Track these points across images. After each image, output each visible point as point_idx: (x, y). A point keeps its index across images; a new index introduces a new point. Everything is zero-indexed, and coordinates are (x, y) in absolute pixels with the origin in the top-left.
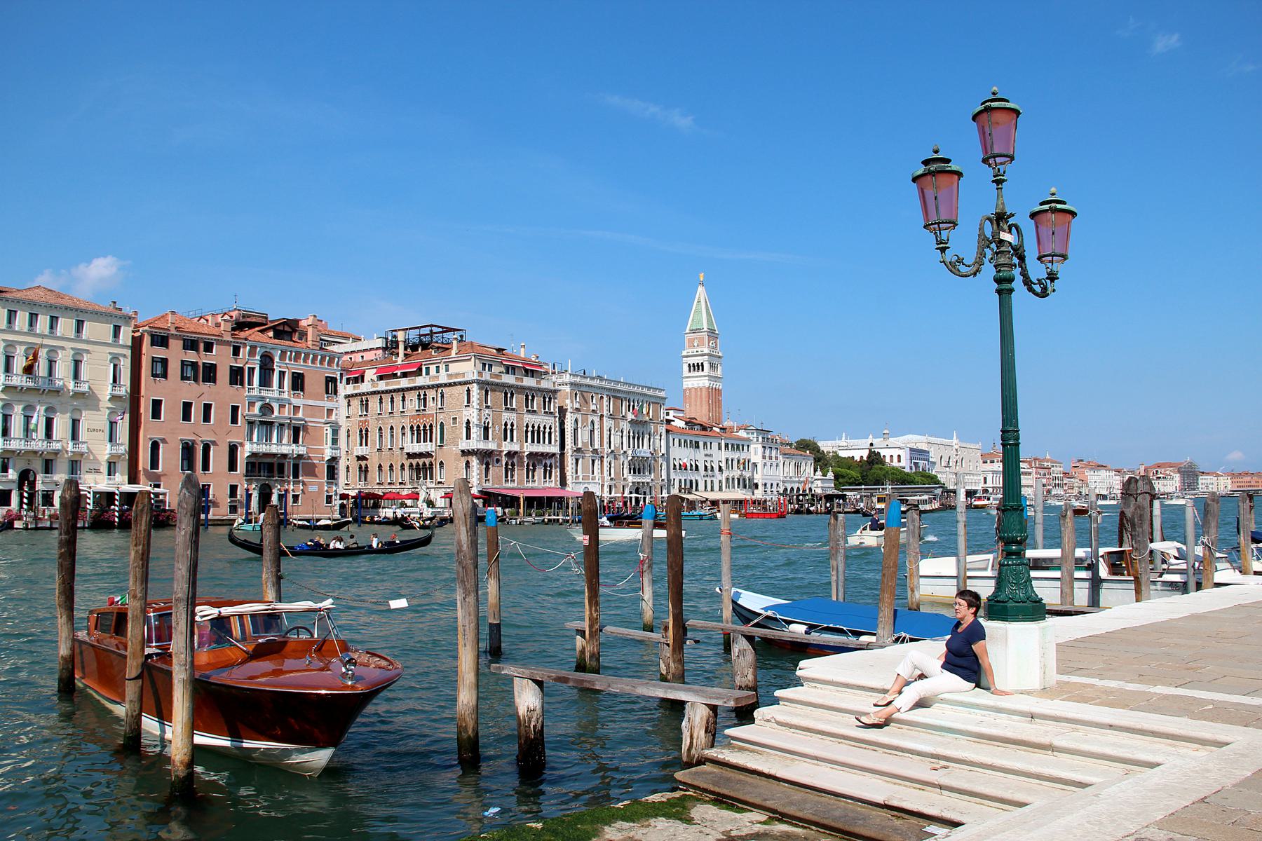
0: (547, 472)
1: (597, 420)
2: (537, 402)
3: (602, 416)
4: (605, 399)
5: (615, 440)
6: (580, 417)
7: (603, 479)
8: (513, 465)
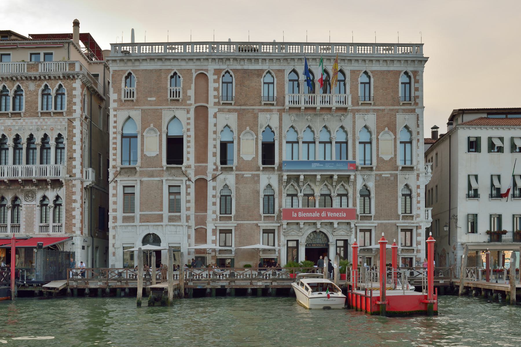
3: (201, 112)
7: (201, 221)
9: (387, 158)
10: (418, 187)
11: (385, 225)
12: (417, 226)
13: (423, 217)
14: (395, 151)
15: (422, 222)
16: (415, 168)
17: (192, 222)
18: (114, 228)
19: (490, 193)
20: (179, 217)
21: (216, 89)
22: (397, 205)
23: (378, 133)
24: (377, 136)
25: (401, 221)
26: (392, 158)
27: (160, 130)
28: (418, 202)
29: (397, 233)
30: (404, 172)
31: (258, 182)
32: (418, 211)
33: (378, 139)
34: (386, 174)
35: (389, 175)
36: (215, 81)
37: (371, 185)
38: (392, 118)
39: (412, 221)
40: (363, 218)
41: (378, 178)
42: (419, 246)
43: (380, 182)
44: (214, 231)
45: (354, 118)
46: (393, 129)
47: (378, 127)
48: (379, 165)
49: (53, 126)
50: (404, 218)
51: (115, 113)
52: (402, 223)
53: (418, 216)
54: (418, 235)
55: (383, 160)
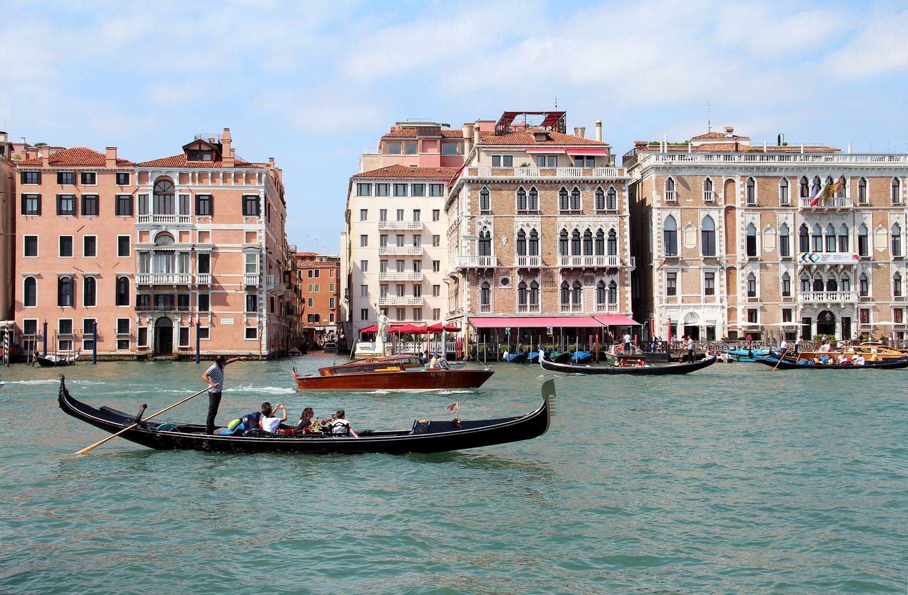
0: (606, 294)
1: (717, 215)
2: (588, 197)
3: (729, 210)
4: (738, 182)
5: (768, 244)
6: (676, 214)
8: (535, 288)
9: (881, 250)
17: (725, 304)
18: (661, 307)
20: (714, 298)
21: (742, 193)
27: (697, 227)
31: (777, 270)
36: (741, 186)
44: (743, 310)
45: (854, 216)
49: (608, 223)
51: (659, 212)
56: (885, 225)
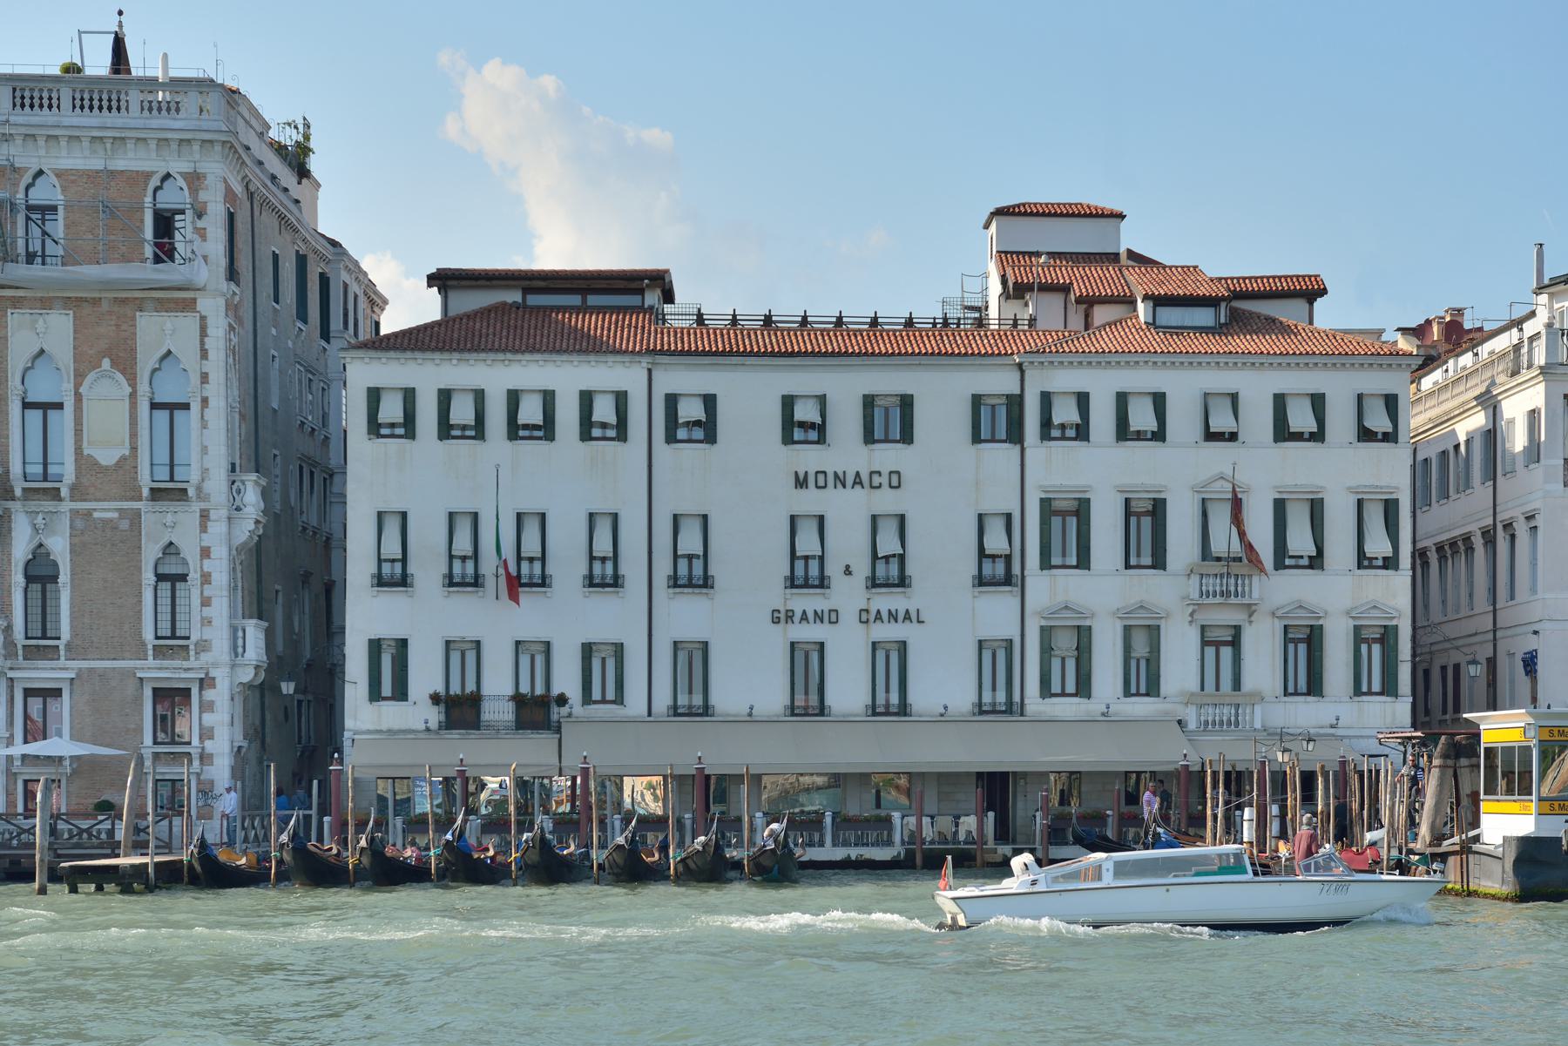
10: (205, 553)
11: (103, 675)
12: (201, 680)
13: (227, 650)
14: (134, 435)
15: (216, 665)
16: (191, 492)
19: (445, 570)
22: (140, 611)
23: (79, 377)
24: (77, 386)
25: (151, 661)
26: (123, 459)
28: (206, 602)
29: (138, 700)
30: (159, 506)
32: (206, 629)
33: (78, 398)
34: (105, 510)
35: (116, 515)
37: (59, 546)
38: (124, 327)
39: (186, 664)
40: (32, 653)
41: (79, 524)
42: (208, 744)
43: (86, 534)
46: (126, 364)
47: (78, 358)
48: (84, 480)
50: (159, 652)
52: (156, 671)
53: (203, 646)
54: (207, 707)
55: (96, 463)
56: (126, 364)
